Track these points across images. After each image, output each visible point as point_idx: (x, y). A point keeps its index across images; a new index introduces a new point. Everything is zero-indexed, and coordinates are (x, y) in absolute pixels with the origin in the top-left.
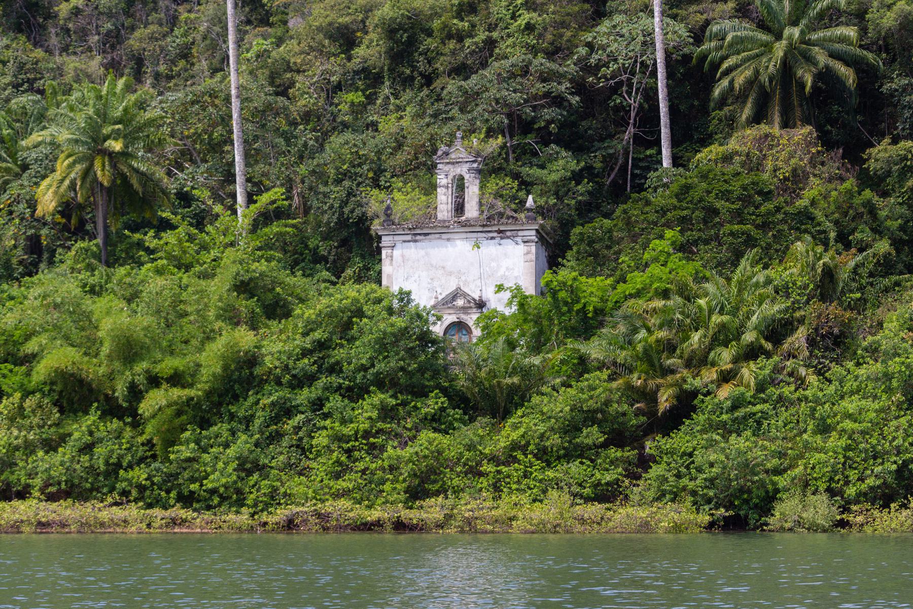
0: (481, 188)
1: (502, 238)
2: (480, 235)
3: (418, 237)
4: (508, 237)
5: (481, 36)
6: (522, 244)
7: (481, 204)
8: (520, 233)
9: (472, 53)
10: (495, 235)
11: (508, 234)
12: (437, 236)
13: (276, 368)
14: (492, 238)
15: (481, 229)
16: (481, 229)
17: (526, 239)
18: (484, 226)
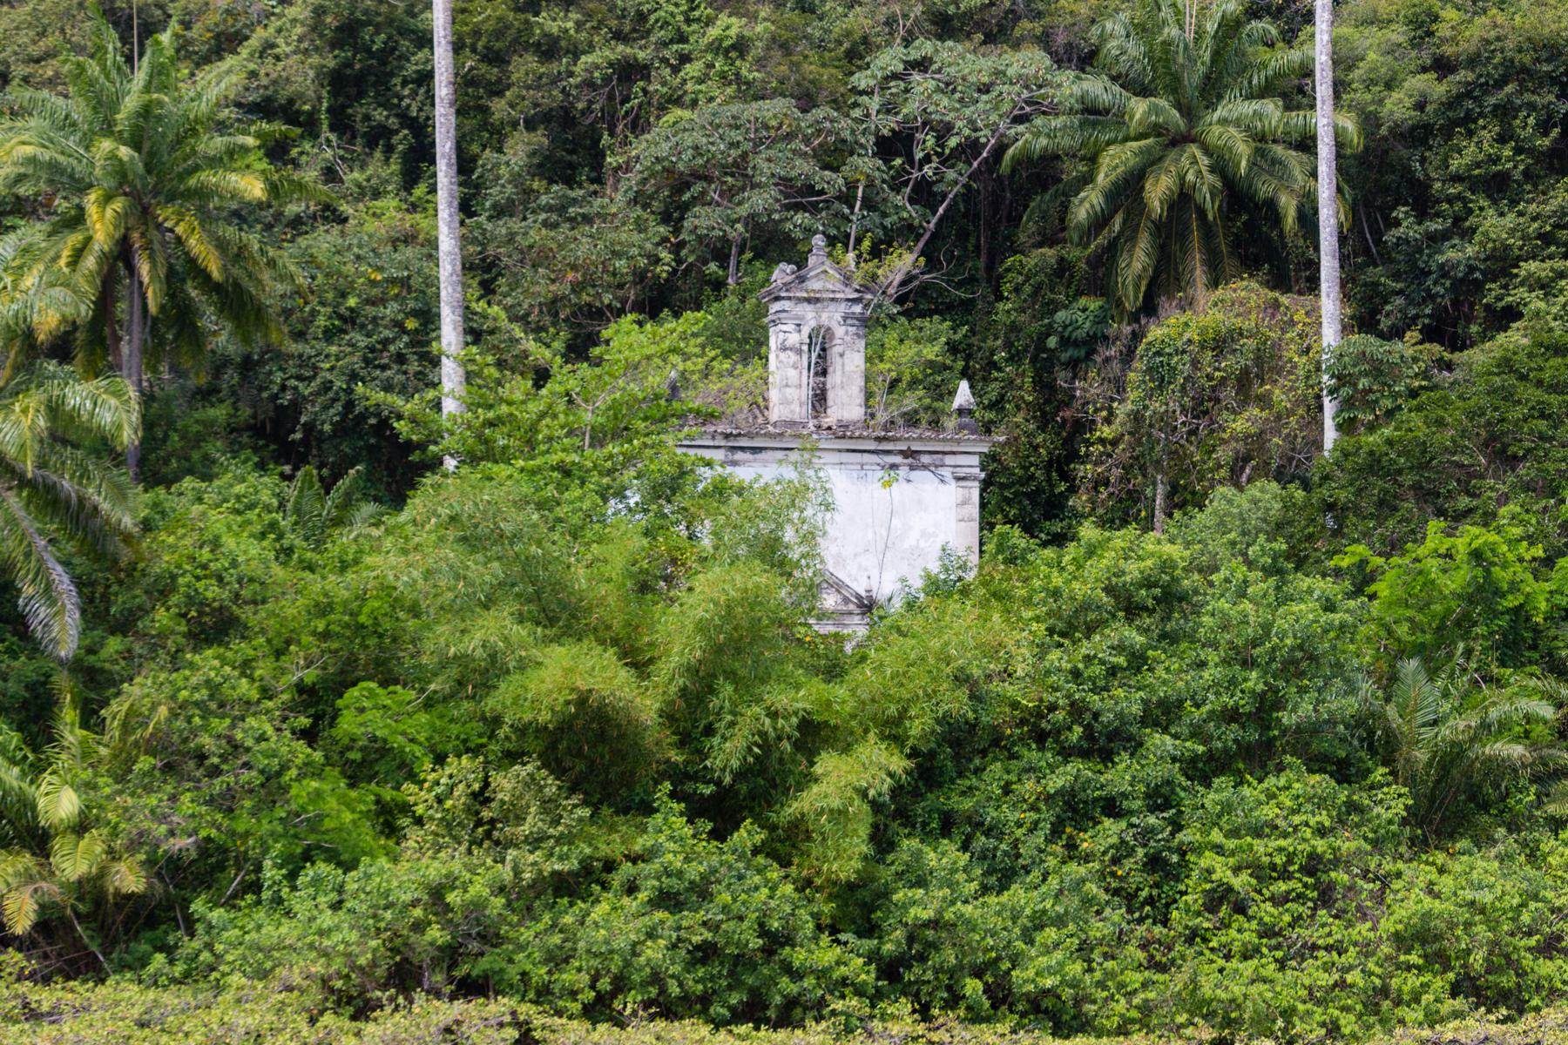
0: (869, 360)
1: (912, 468)
2: (867, 458)
3: (739, 456)
4: (925, 467)
5: (601, 57)
6: (953, 482)
7: (869, 395)
8: (949, 460)
9: (589, 84)
10: (898, 459)
11: (925, 459)
12: (779, 455)
13: (1053, 708)
14: (893, 466)
15: (872, 446)
16: (872, 446)
17: (962, 472)
18: (878, 439)
